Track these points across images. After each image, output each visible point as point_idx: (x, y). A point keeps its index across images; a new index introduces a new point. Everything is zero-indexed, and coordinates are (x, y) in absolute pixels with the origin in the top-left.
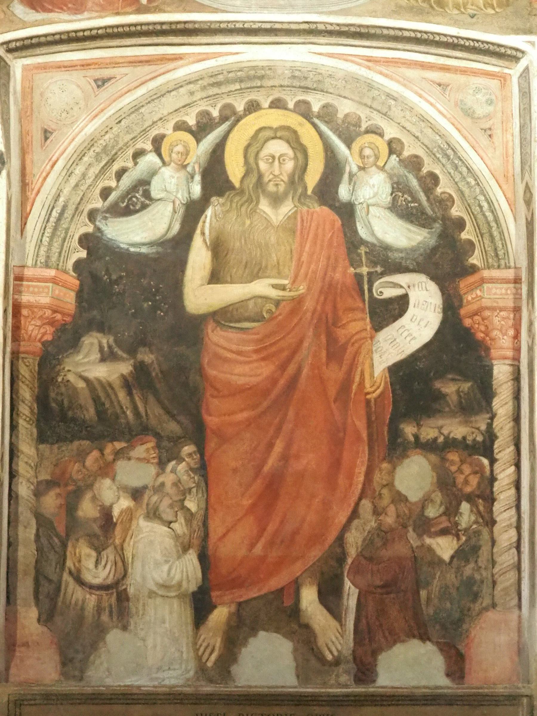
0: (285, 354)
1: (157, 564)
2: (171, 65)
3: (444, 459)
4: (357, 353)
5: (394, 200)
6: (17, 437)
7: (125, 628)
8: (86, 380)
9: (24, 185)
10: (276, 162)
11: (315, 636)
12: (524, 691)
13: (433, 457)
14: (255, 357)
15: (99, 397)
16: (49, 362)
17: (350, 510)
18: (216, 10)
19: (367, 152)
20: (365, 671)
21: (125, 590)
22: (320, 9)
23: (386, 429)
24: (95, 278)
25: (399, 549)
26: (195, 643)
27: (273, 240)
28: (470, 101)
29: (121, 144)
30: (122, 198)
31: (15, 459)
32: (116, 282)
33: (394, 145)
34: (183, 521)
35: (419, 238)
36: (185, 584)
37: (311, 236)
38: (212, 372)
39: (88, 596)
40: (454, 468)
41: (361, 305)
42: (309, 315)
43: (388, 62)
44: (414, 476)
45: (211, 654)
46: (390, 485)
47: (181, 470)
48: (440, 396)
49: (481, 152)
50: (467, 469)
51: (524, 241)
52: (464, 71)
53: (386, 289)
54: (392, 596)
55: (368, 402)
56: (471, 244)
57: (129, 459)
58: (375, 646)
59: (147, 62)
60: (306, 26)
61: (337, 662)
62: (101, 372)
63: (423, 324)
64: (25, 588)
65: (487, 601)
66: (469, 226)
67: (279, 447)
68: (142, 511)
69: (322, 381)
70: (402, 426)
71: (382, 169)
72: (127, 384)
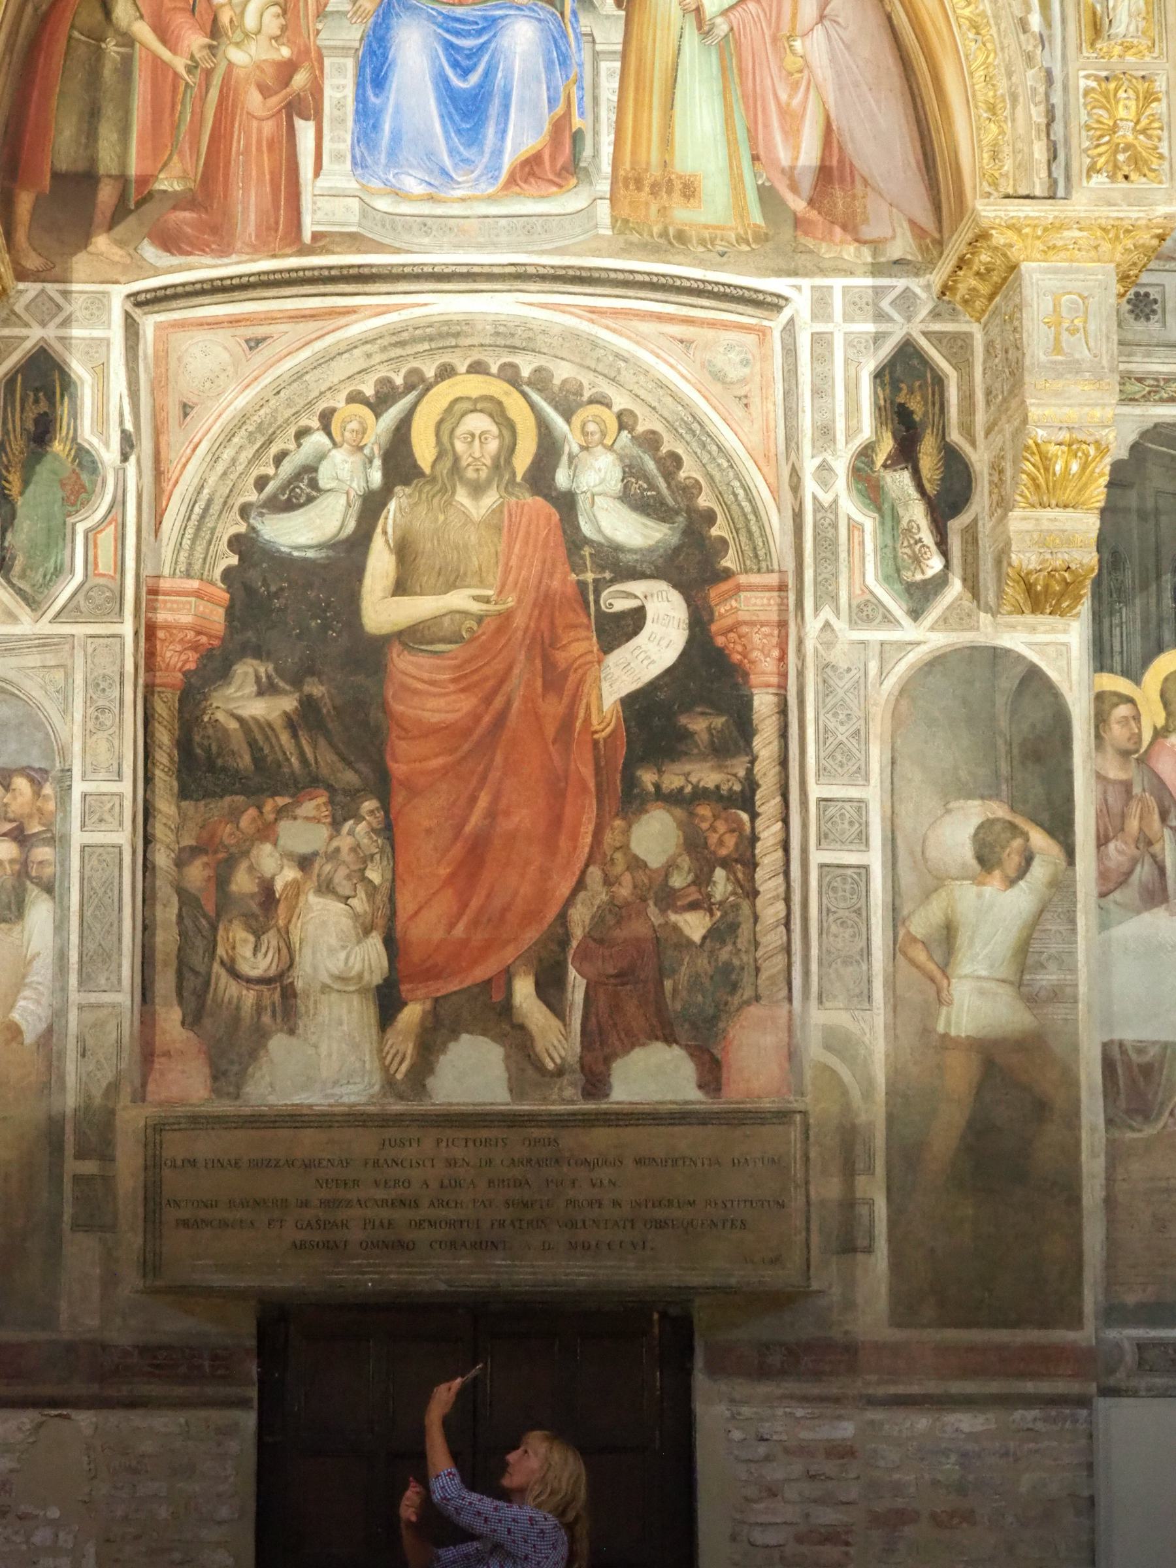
0: (491, 683)
1: (332, 951)
2: (343, 321)
3: (692, 814)
4: (581, 682)
5: (626, 487)
6: (153, 792)
7: (292, 1032)
8: (239, 719)
9: (158, 474)
10: (477, 441)
11: (532, 1039)
12: (796, 1106)
13: (679, 812)
14: (452, 687)
15: (256, 741)
16: (192, 696)
17: (575, 879)
18: (398, 251)
19: (591, 427)
20: (595, 1082)
21: (292, 983)
22: (530, 248)
23: (619, 776)
24: (249, 590)
25: (637, 928)
26: (380, 1050)
27: (474, 539)
28: (720, 361)
29: (280, 421)
30: (282, 489)
31: (151, 820)
32: (276, 595)
33: (625, 419)
35: (658, 536)
36: (367, 976)
37: (521, 534)
38: (398, 708)
39: (244, 992)
40: (705, 826)
41: (585, 621)
42: (520, 634)
43: (616, 313)
44: (654, 836)
45: (400, 1064)
46: (625, 847)
47: (360, 832)
48: (686, 735)
49: (734, 425)
50: (721, 827)
51: (790, 538)
52: (712, 324)
53: (616, 600)
54: (629, 987)
55: (596, 743)
56: (723, 541)
57: (295, 818)
58: (607, 1050)
59: (312, 316)
60: (512, 270)
61: (560, 1072)
62: (257, 709)
63: (664, 643)
64: (165, 982)
65: (748, 993)
66: (720, 519)
67: (483, 801)
68: (311, 884)
69: (538, 717)
70: (639, 773)
71: (610, 448)
72: (291, 724)
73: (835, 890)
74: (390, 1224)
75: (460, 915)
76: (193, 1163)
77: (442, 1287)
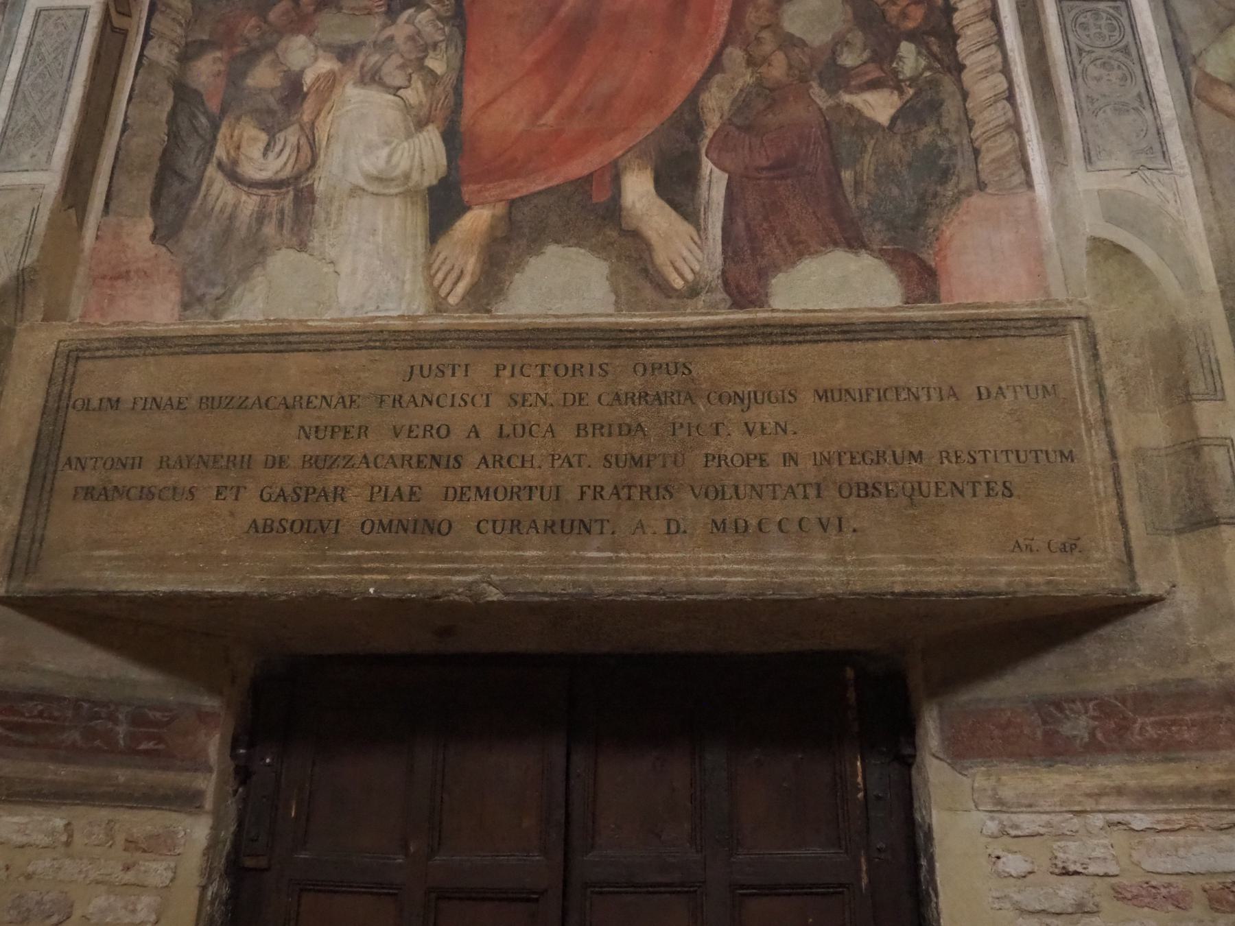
1: (370, 148)
7: (302, 246)
11: (648, 246)
17: (707, 62)
26: (428, 266)
34: (420, 85)
36: (415, 176)
39: (244, 197)
45: (455, 284)
46: (773, 26)
54: (789, 181)
58: (763, 262)
73: (1084, 26)
74: (412, 493)
75: (550, 103)
76: (115, 403)
77: (494, 595)
